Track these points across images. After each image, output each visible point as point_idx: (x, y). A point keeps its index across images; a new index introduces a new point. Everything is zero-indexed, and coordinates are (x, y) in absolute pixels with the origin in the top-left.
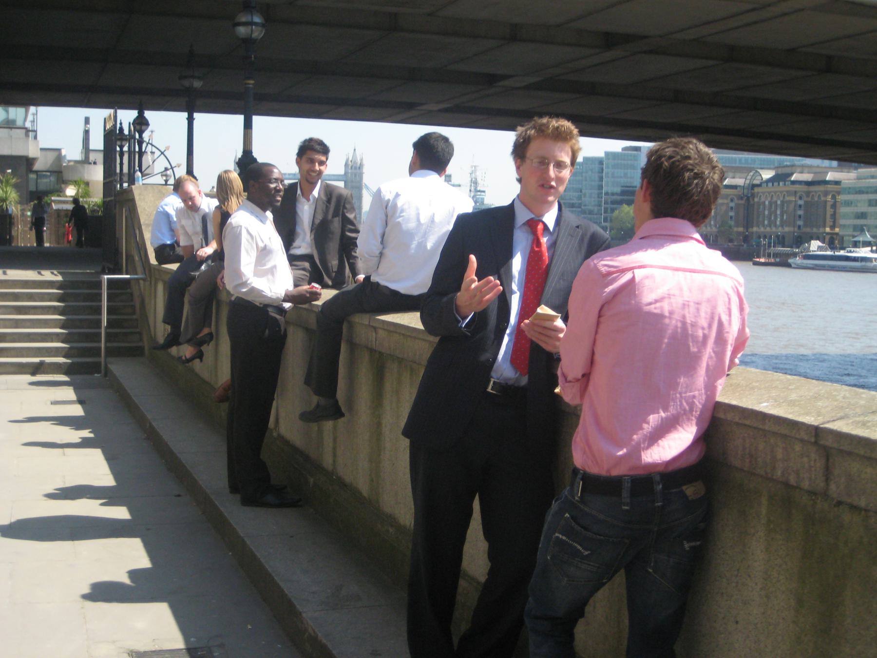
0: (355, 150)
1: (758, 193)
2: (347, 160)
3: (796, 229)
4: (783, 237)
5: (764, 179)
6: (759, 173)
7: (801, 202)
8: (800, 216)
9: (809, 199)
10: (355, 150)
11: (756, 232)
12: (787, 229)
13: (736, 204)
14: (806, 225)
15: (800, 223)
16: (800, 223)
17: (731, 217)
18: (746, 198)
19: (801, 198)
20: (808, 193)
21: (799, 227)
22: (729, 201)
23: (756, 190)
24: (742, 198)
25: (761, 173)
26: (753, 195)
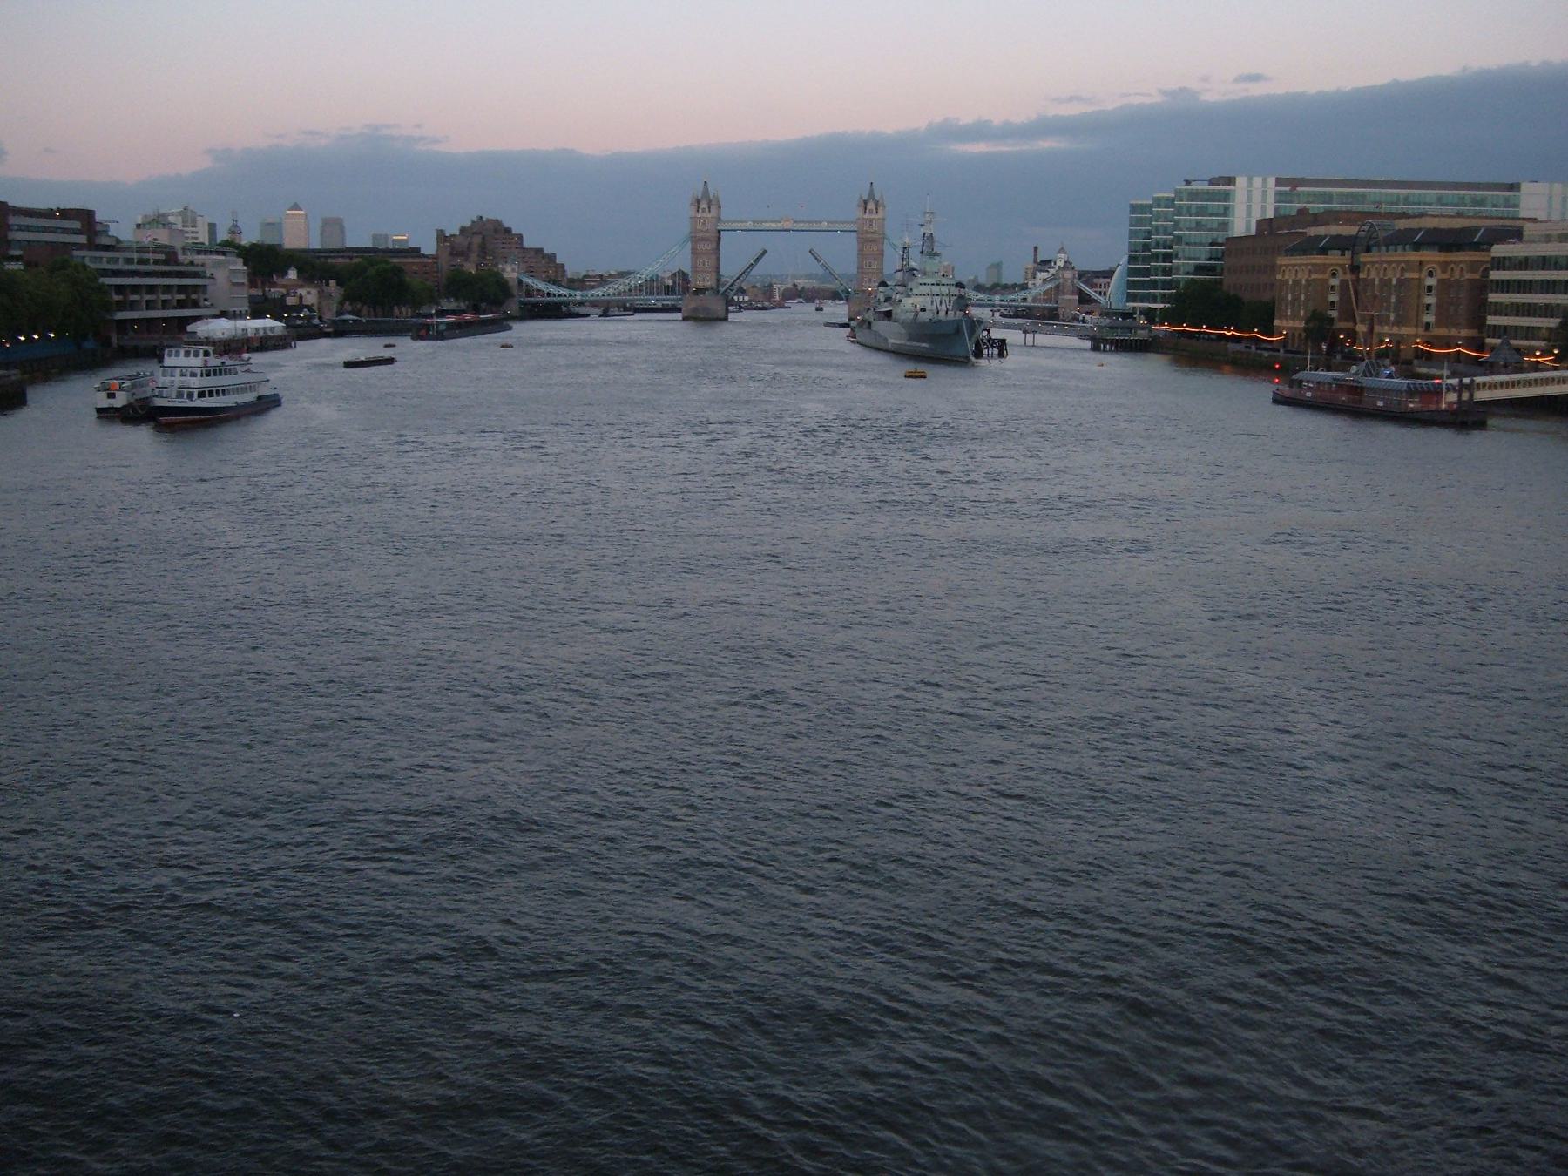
7: (1431, 282)
9: (1445, 276)
16: (1430, 318)
17: (1333, 303)
19: (1431, 274)
20: (1444, 266)
21: (1428, 326)
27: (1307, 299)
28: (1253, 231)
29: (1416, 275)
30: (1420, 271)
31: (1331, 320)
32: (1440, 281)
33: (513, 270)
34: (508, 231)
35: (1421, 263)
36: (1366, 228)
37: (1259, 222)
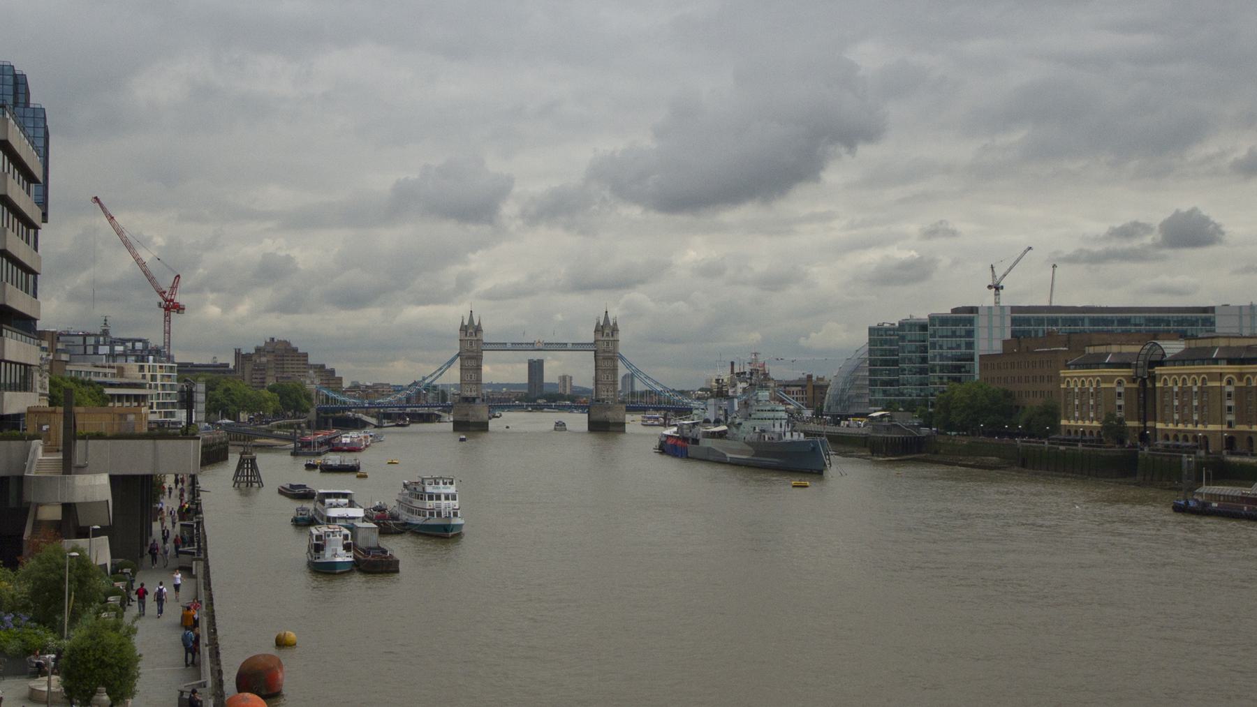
0: (607, 312)
1: (1161, 375)
2: (598, 324)
3: (1225, 427)
4: (1205, 437)
5: (1168, 356)
6: (1159, 345)
7: (1230, 389)
8: (1230, 408)
9: (1243, 384)
10: (607, 312)
11: (1162, 430)
12: (1211, 427)
13: (1126, 389)
14: (1240, 422)
15: (1231, 418)
16: (1231, 418)
17: (1120, 407)
18: (1140, 379)
20: (1240, 376)
21: (1230, 424)
22: (1114, 385)
23: (1158, 370)
24: (1134, 381)
25: (1163, 346)
26: (1153, 378)
27: (1097, 405)
28: (997, 348)
29: (1217, 384)
30: (1221, 380)
31: (1120, 421)
32: (1237, 388)
33: (312, 383)
34: (295, 350)
35: (1221, 374)
36: (1148, 347)
37: (1005, 342)
